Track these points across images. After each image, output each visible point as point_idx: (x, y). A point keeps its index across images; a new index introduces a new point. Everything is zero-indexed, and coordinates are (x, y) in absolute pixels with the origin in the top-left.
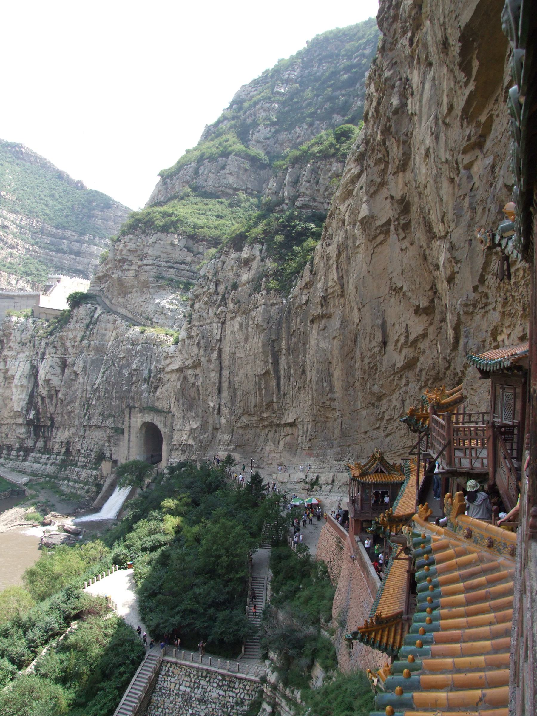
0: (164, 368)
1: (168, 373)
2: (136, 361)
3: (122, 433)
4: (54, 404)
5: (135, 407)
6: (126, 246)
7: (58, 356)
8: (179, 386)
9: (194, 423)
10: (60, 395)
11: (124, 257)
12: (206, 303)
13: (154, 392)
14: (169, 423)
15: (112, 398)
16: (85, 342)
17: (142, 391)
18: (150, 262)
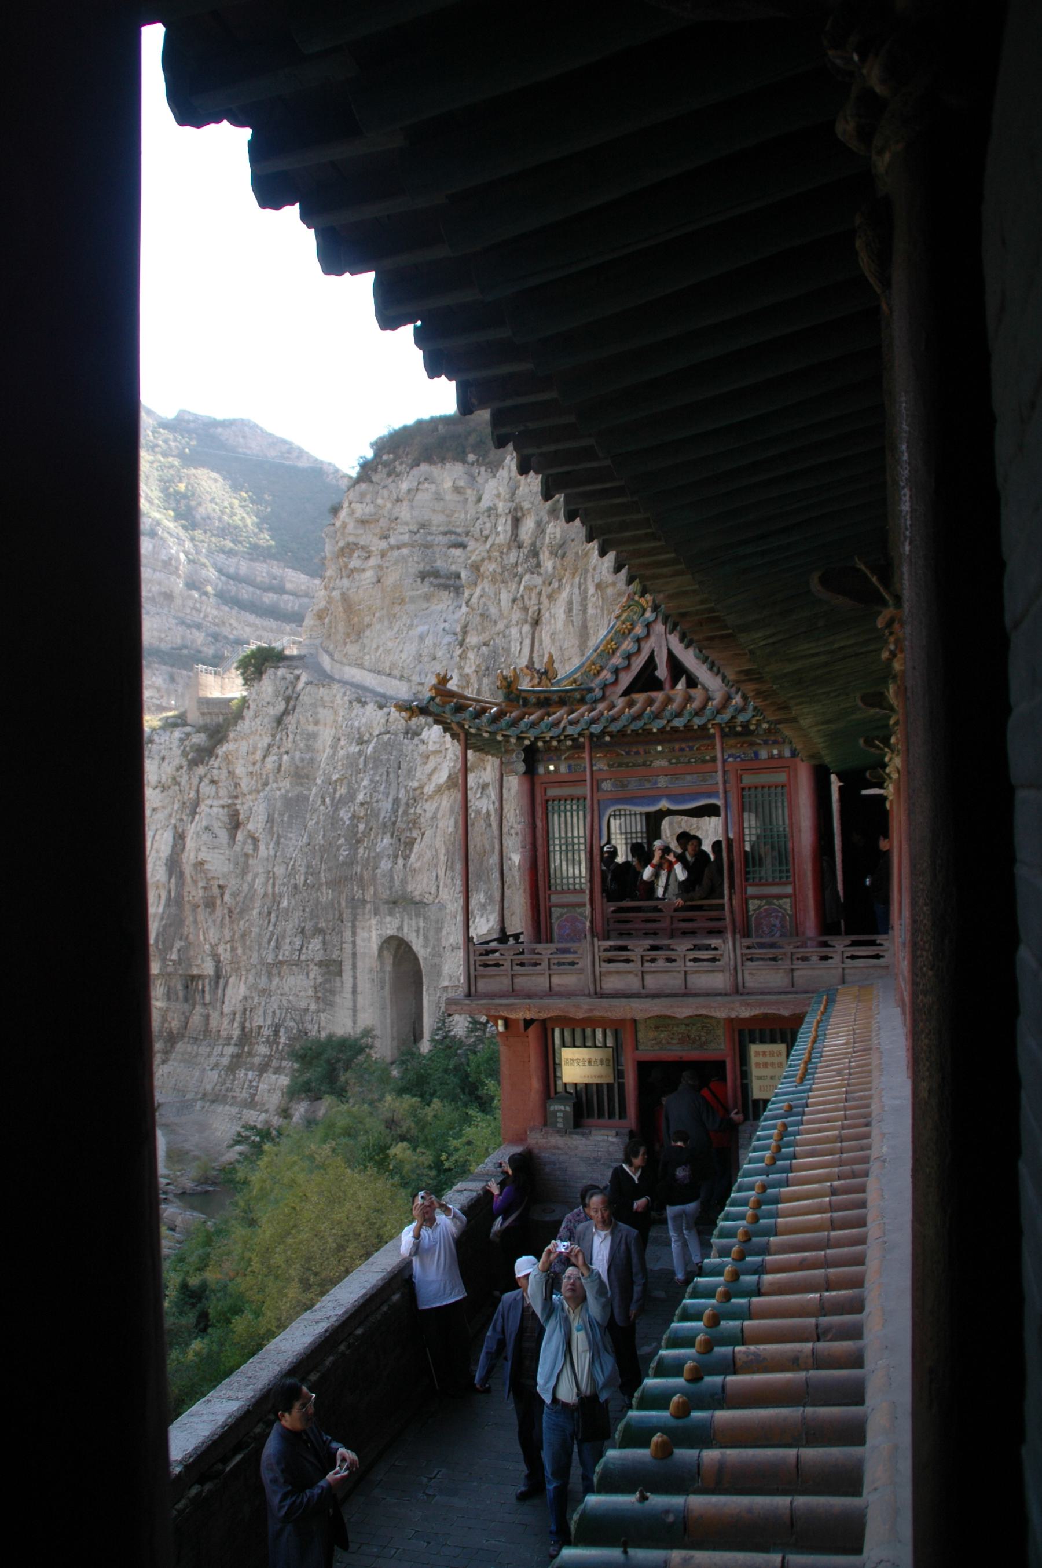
0: (422, 787)
1: (431, 797)
2: (365, 783)
3: (340, 973)
4: (219, 920)
5: (364, 902)
6: (352, 512)
7: (221, 802)
8: (450, 830)
9: (484, 920)
10: (226, 897)
11: (351, 539)
12: (494, 581)
13: (406, 858)
14: (431, 934)
15: (321, 885)
16: (271, 759)
17: (378, 857)
18: (406, 538)
